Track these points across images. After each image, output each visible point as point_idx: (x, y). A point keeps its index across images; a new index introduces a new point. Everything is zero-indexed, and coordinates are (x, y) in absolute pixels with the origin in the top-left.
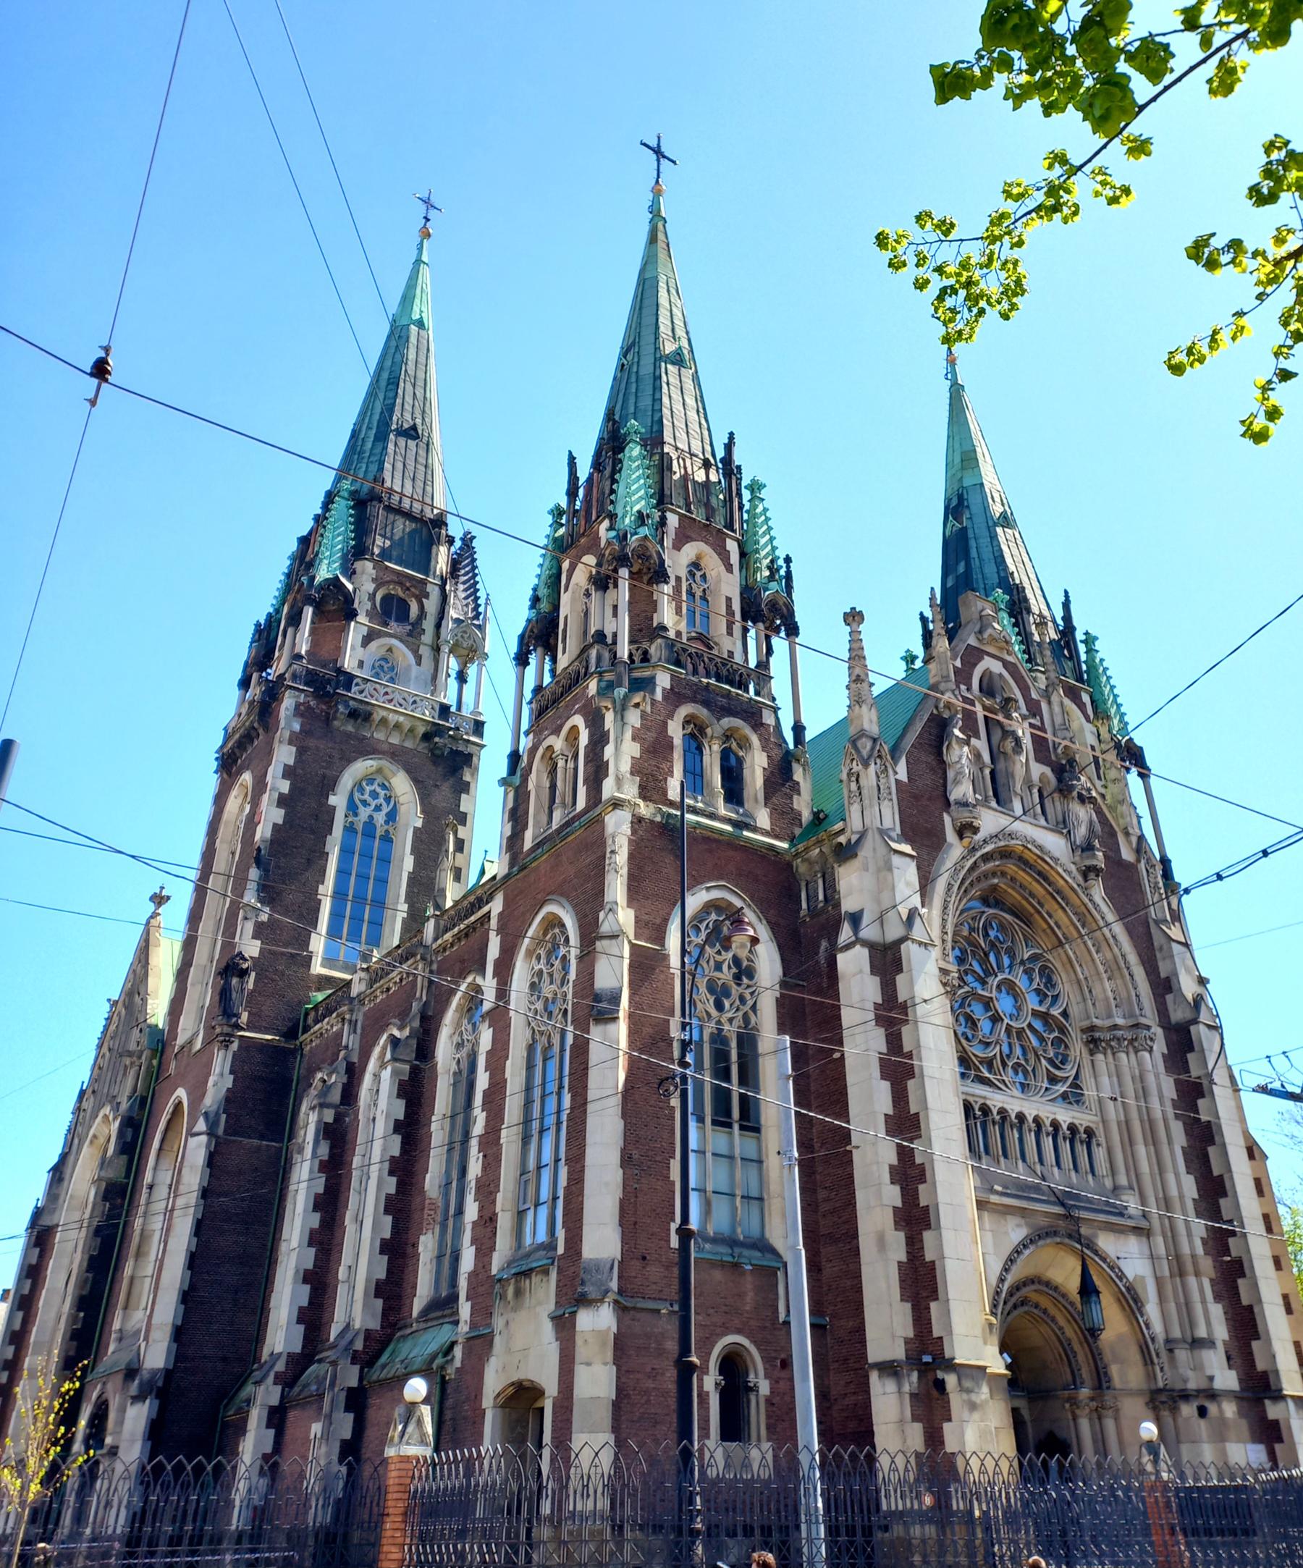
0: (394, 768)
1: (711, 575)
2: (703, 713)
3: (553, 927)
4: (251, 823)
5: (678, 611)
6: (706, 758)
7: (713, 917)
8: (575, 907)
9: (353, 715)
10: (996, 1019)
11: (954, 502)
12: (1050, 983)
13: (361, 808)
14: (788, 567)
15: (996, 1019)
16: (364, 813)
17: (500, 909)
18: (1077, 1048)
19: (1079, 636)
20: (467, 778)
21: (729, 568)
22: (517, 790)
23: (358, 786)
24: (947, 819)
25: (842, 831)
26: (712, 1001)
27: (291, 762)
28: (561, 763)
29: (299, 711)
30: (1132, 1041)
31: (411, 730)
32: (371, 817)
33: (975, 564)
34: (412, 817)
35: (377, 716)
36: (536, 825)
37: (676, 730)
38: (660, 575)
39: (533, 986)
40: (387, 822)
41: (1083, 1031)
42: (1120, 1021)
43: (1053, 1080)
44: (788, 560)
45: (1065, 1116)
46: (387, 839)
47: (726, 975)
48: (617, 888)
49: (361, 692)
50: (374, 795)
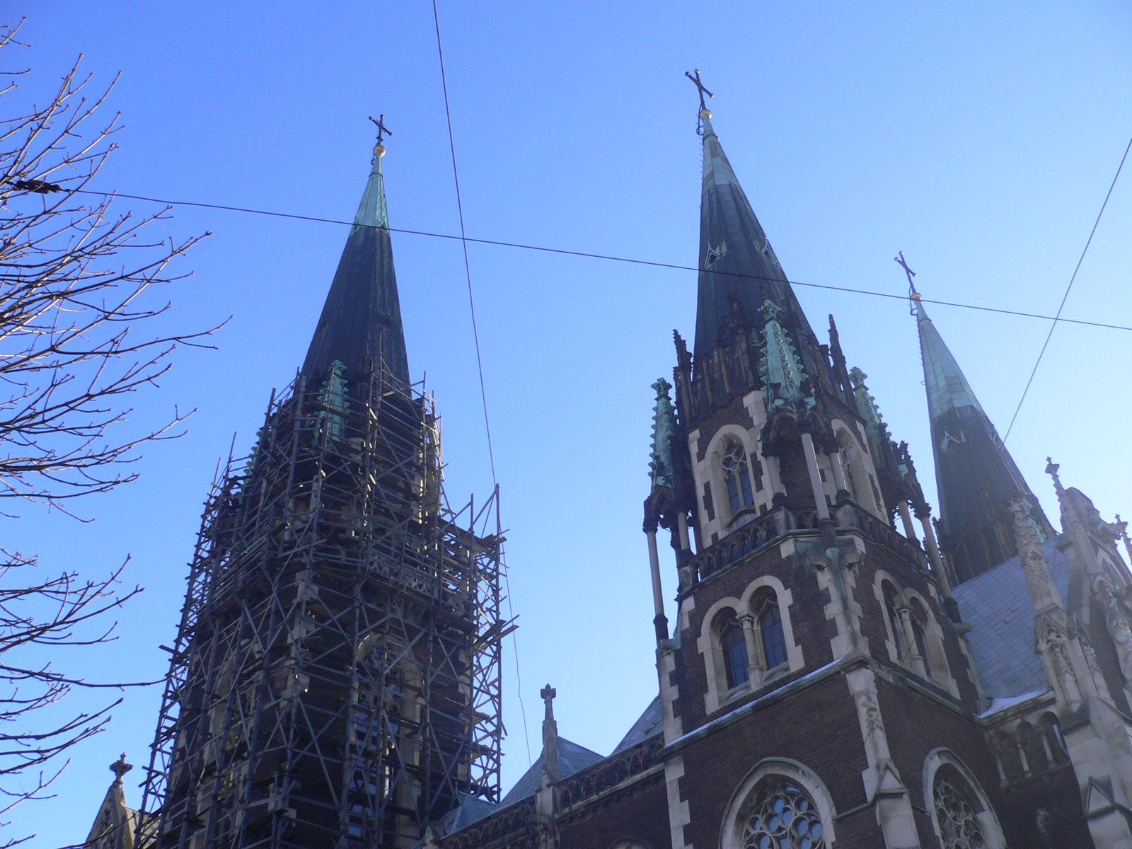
3: (774, 789)
6: (896, 624)
7: (944, 783)
17: (681, 773)
22: (678, 655)
28: (746, 625)
36: (719, 686)
48: (877, 746)
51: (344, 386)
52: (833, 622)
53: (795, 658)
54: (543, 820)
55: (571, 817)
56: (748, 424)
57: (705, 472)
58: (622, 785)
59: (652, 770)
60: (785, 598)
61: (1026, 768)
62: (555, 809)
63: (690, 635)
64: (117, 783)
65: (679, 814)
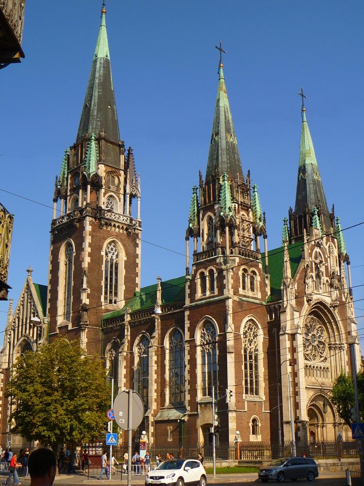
2: (246, 267)
4: (79, 260)
9: (106, 224)
11: (303, 168)
12: (322, 333)
13: (109, 255)
16: (110, 255)
18: (327, 349)
19: (336, 218)
20: (137, 242)
24: (305, 298)
26: (249, 344)
27: (90, 242)
28: (207, 278)
29: (91, 224)
31: (123, 227)
33: (308, 193)
34: (123, 257)
35: (113, 224)
37: (240, 273)
38: (237, 228)
39: (201, 336)
40: (116, 258)
41: (329, 345)
43: (321, 357)
44: (264, 214)
45: (323, 365)
46: (117, 264)
49: (107, 215)
51: (95, 144)
52: (225, 284)
59: (182, 309)
65: (187, 324)
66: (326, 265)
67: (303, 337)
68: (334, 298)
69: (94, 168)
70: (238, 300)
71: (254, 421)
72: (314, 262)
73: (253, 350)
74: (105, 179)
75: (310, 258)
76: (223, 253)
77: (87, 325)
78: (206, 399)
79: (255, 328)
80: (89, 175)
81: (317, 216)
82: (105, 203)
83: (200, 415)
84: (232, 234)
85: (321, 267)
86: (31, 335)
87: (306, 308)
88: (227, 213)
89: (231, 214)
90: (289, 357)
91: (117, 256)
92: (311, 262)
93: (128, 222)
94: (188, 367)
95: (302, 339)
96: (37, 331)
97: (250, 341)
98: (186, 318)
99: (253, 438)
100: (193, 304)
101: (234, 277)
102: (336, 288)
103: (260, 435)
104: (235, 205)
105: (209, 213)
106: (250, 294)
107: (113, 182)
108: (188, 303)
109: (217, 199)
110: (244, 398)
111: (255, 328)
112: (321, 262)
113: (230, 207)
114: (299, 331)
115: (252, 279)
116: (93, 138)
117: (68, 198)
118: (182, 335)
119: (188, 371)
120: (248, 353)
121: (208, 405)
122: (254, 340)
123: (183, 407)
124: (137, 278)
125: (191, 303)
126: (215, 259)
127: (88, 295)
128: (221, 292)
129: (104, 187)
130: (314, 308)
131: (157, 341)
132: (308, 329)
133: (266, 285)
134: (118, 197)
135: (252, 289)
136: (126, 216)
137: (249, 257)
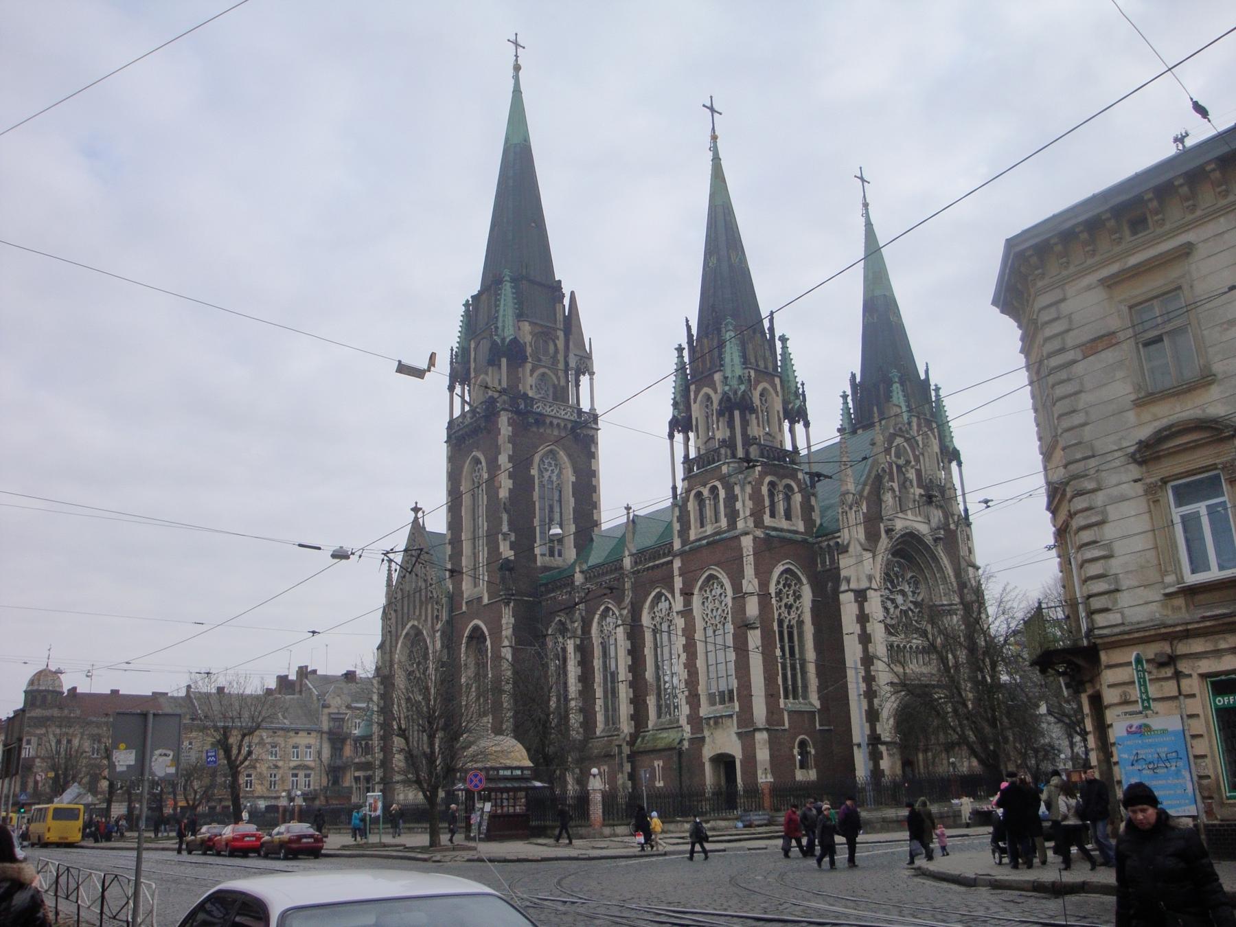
0: (558, 449)
1: (769, 399)
5: (759, 425)
7: (785, 576)
8: (727, 574)
10: (896, 607)
12: (917, 588)
14: (803, 388)
15: (896, 607)
16: (546, 475)
19: (933, 387)
20: (593, 450)
21: (778, 396)
22: (680, 507)
23: (542, 460)
24: (882, 526)
25: (839, 537)
28: (707, 502)
30: (949, 611)
31: (565, 425)
32: (550, 477)
34: (570, 476)
35: (548, 421)
36: (696, 527)
37: (765, 490)
38: (753, 410)
39: (703, 603)
42: (945, 603)
44: (803, 384)
47: (791, 599)
48: (749, 570)
49: (538, 407)
50: (550, 464)
51: (512, 288)
53: (724, 523)
54: (626, 572)
55: (638, 571)
56: (716, 392)
57: (696, 411)
58: (657, 562)
60: (722, 494)
61: (828, 563)
62: (632, 568)
63: (686, 501)
64: (416, 519)
65: (678, 583)
66: (918, 467)
67: (882, 596)
68: (934, 525)
69: (511, 329)
70: (762, 536)
71: (803, 744)
72: (896, 464)
73: (794, 622)
74: (531, 346)
75: (888, 457)
76: (734, 456)
77: (513, 595)
78: (715, 711)
79: (795, 584)
80: (503, 340)
81: (898, 385)
82: (534, 387)
83: (707, 740)
84: (745, 424)
85: (907, 471)
86: (423, 618)
87: (884, 543)
88: (736, 387)
89: (743, 387)
90: (857, 629)
91: (559, 476)
92: (890, 465)
93: (574, 417)
94: (684, 657)
95: (879, 599)
96: (432, 611)
97: (789, 607)
98: (676, 572)
99: (800, 775)
100: (687, 548)
101: (756, 497)
102: (937, 507)
103: (814, 770)
104: (749, 372)
105: (706, 390)
106: (784, 524)
107: (546, 352)
108: (677, 545)
109: (718, 364)
110: (782, 706)
111: (795, 584)
112: (908, 462)
113: (740, 376)
114: (874, 586)
115: (788, 498)
116: (508, 278)
117: (473, 381)
118: (670, 603)
119: (684, 664)
120: (785, 627)
121: (720, 720)
122: (795, 605)
123: (678, 727)
124: (595, 511)
125: (683, 547)
126: (719, 467)
127: (511, 543)
128: (732, 523)
129: (530, 360)
130: (901, 542)
131: (630, 615)
132: (890, 578)
133: (812, 509)
134: (556, 375)
135: (788, 516)
136: (571, 407)
137: (779, 461)
